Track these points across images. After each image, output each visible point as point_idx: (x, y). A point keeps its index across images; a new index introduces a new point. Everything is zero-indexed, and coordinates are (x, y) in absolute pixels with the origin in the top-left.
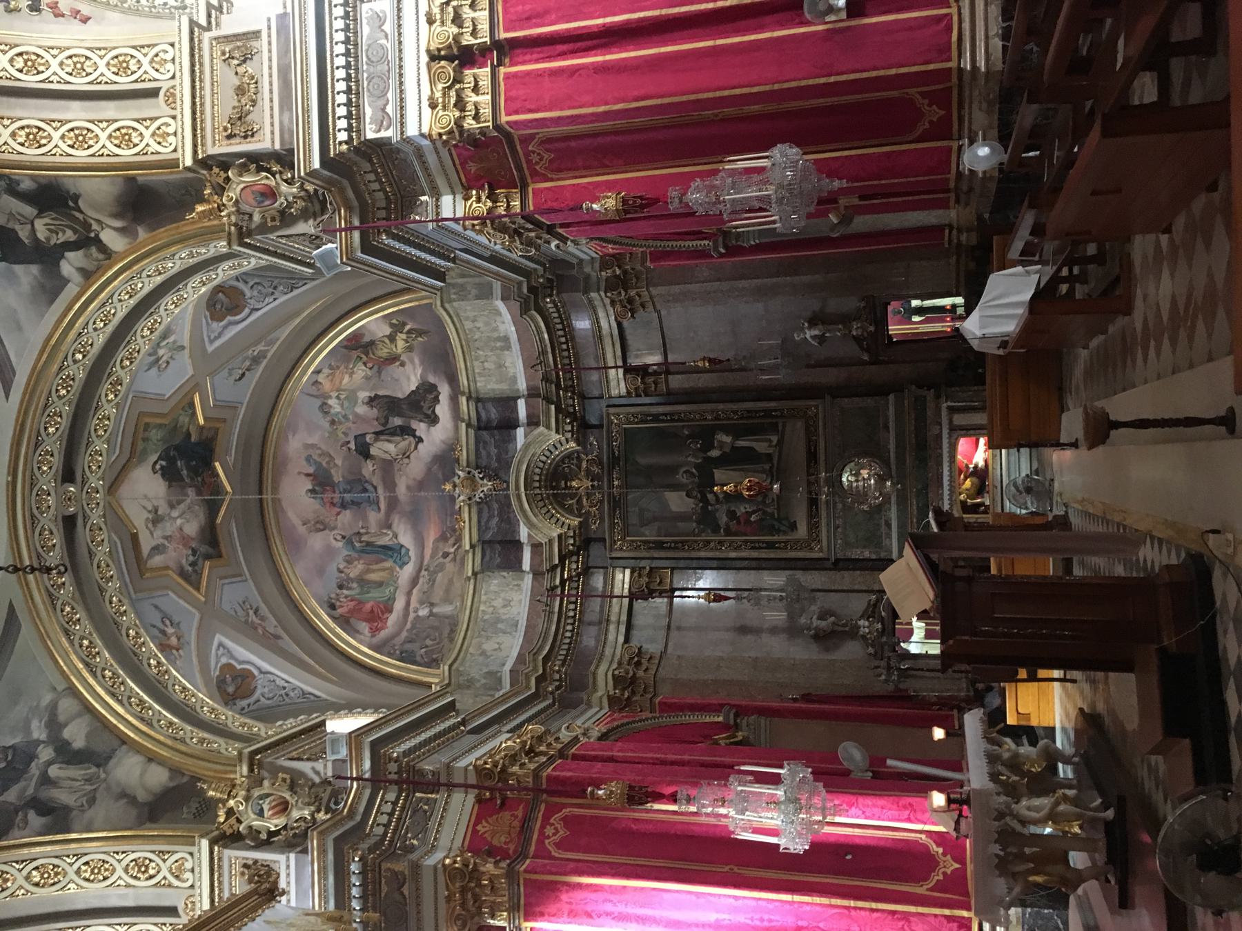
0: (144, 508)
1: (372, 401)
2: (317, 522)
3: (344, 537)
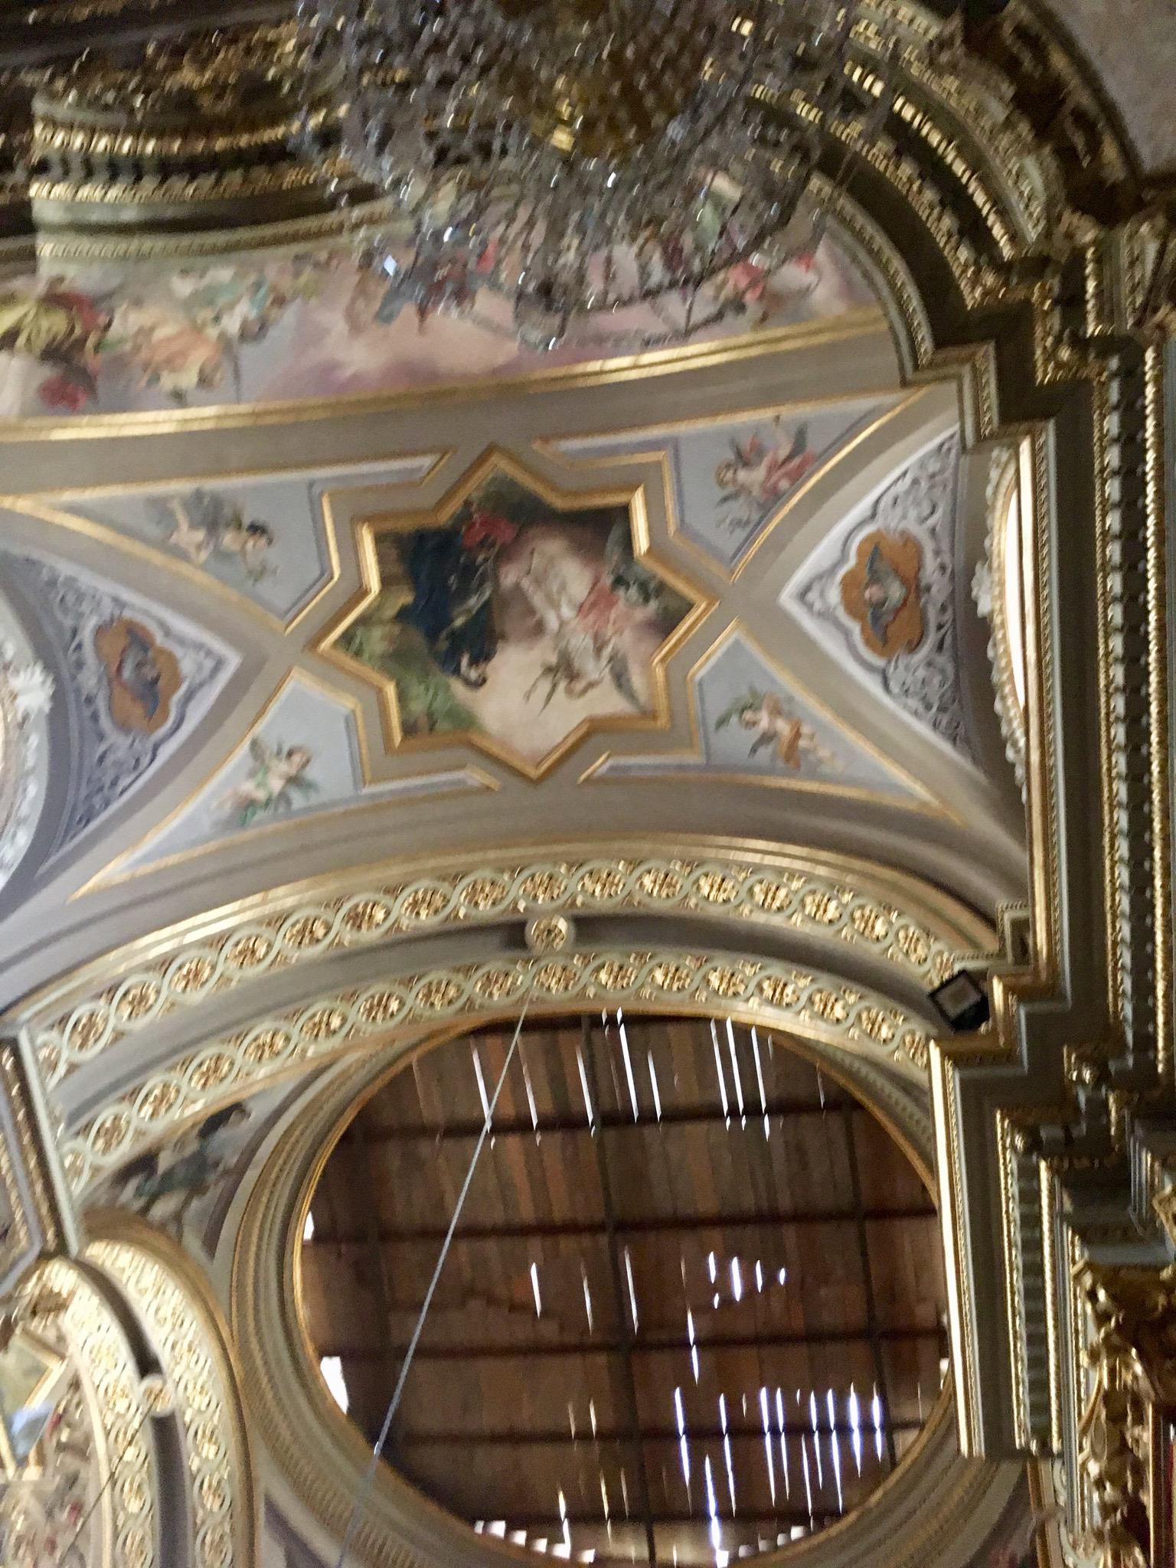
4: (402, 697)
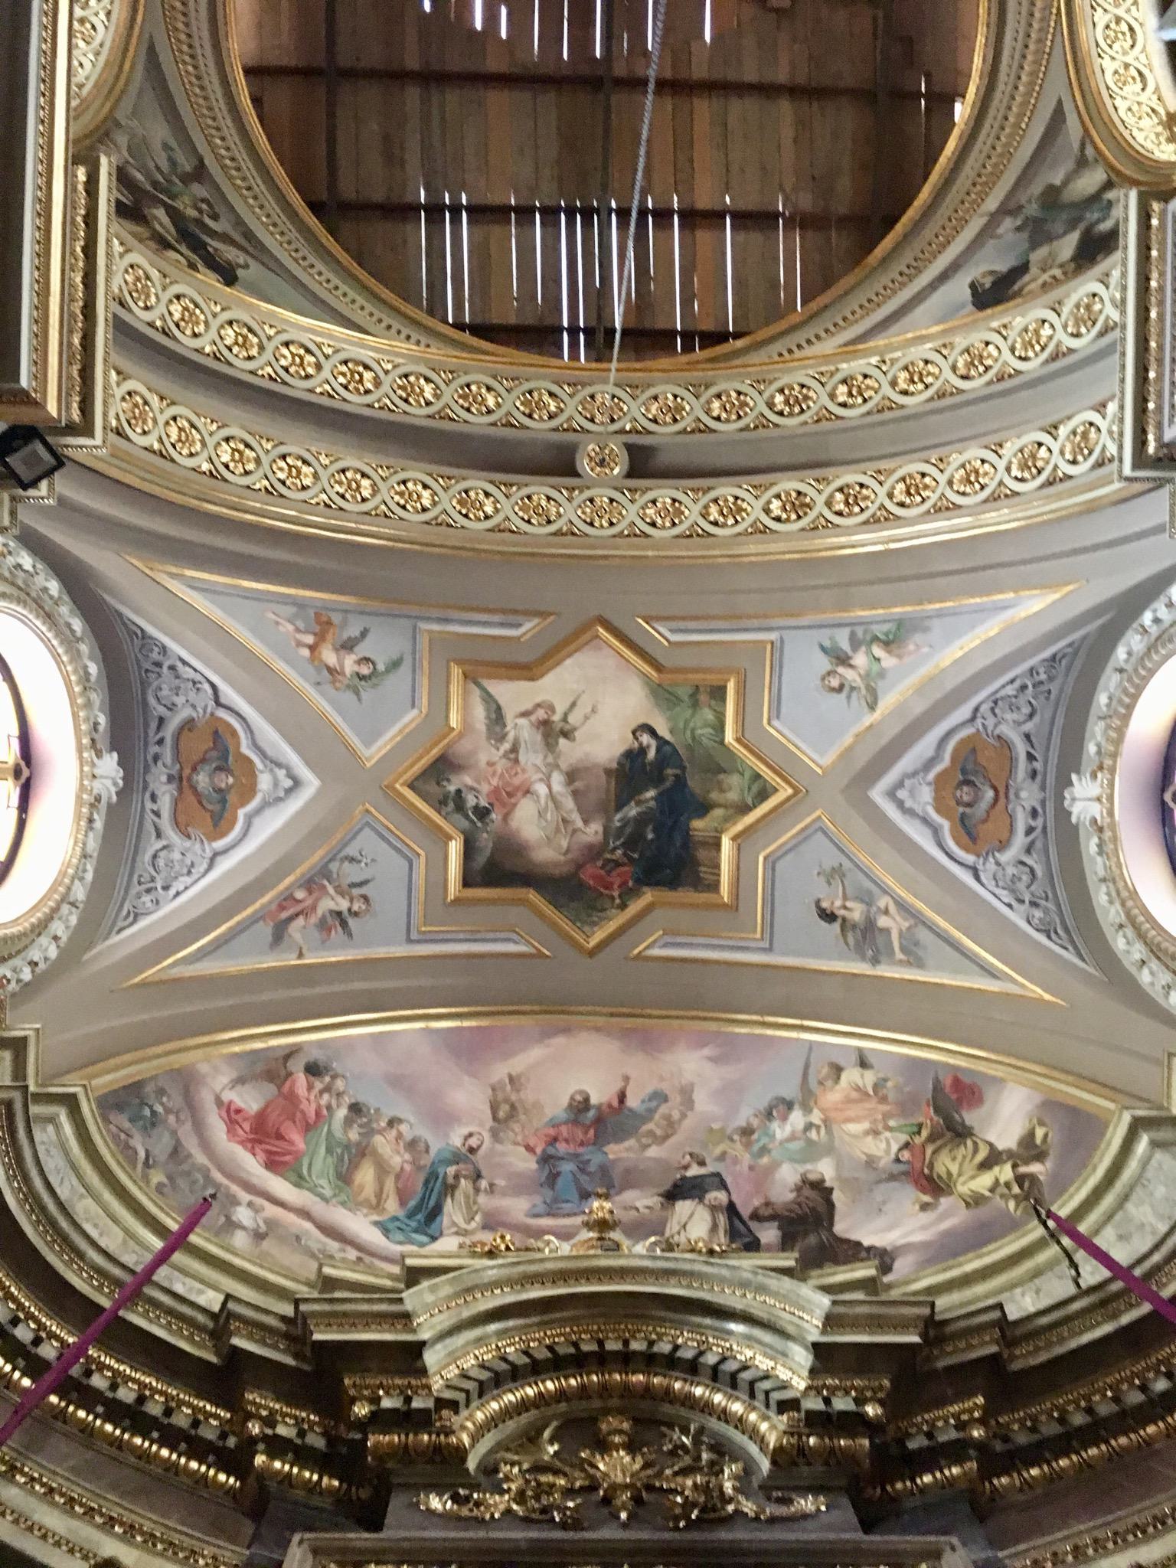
0: (573, 705)
1: (819, 1186)
2: (513, 1107)
3: (472, 1150)
4: (720, 728)
